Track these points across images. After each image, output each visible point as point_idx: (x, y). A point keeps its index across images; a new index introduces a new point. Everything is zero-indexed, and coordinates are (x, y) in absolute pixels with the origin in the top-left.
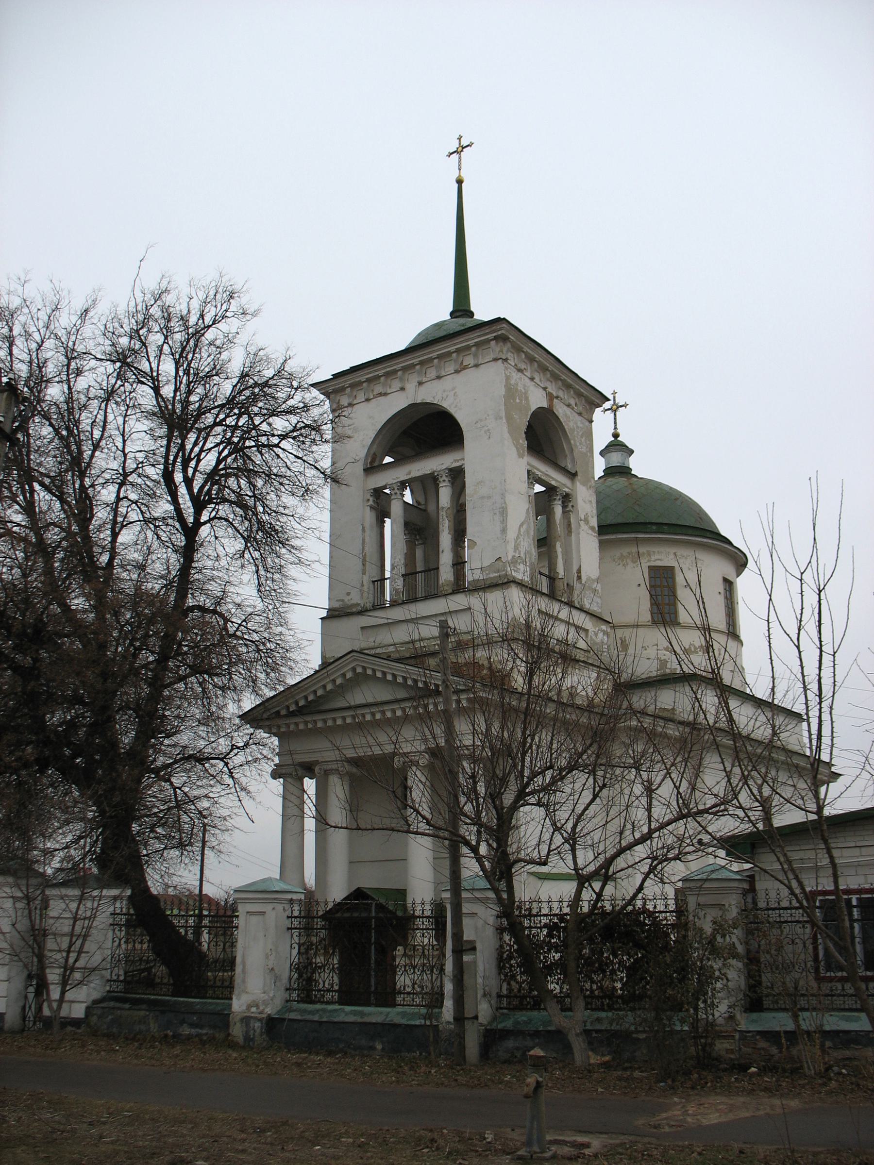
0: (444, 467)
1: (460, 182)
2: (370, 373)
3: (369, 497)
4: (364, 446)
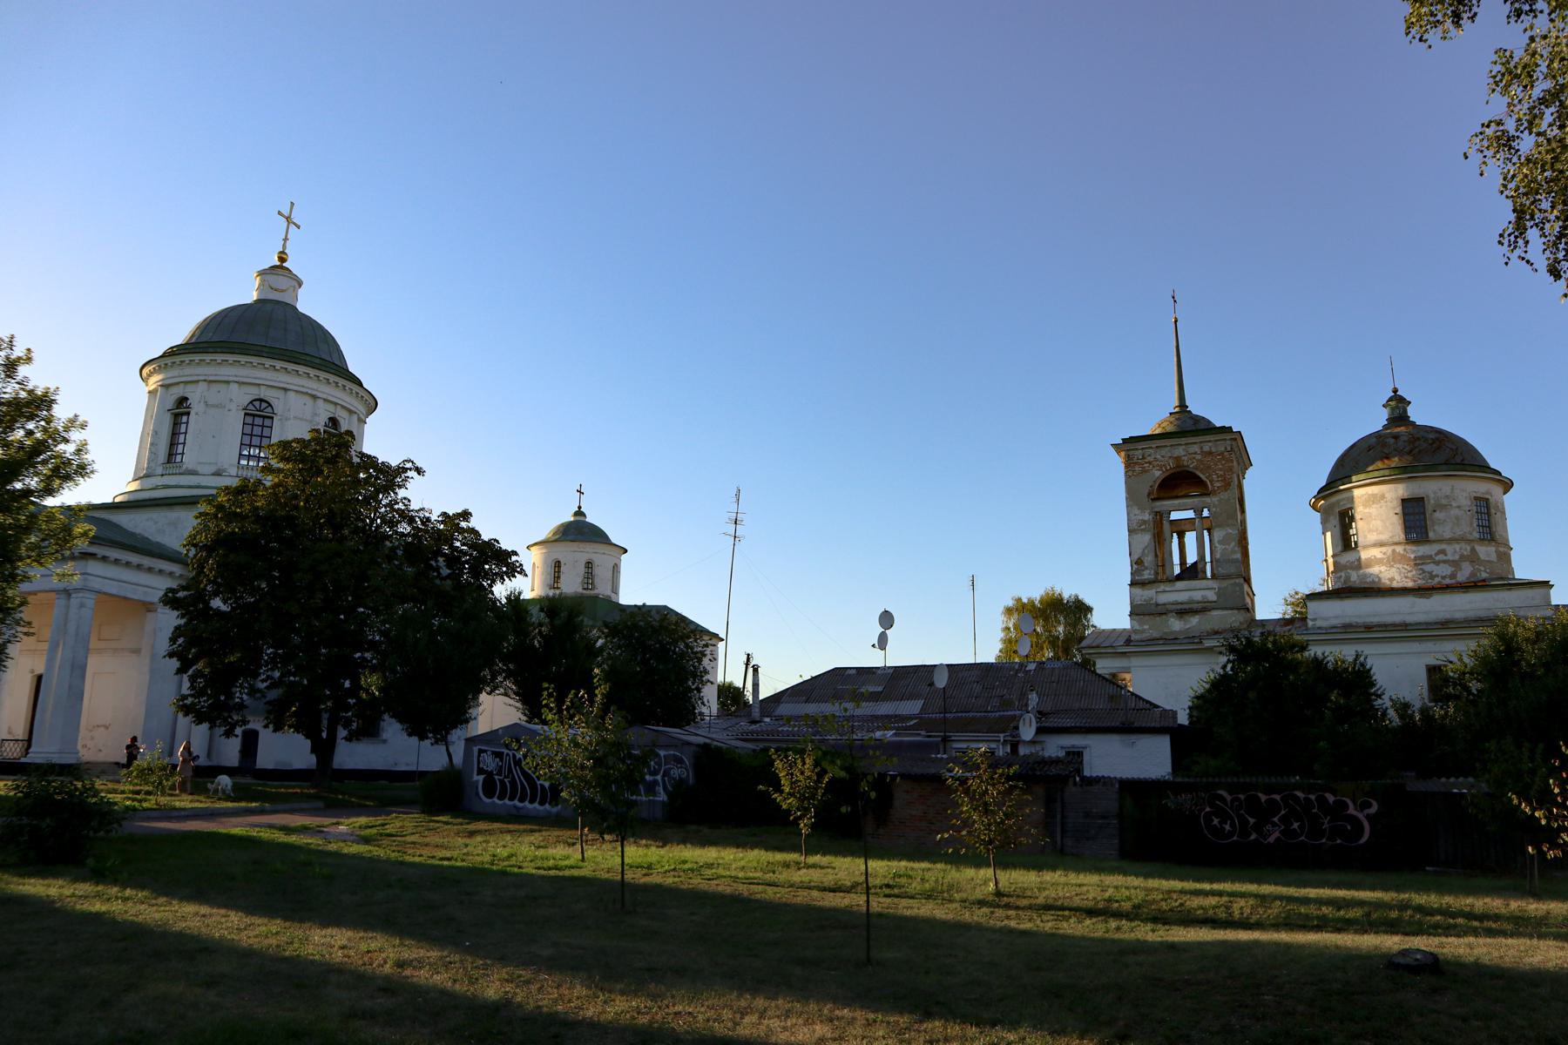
1: (1176, 321)
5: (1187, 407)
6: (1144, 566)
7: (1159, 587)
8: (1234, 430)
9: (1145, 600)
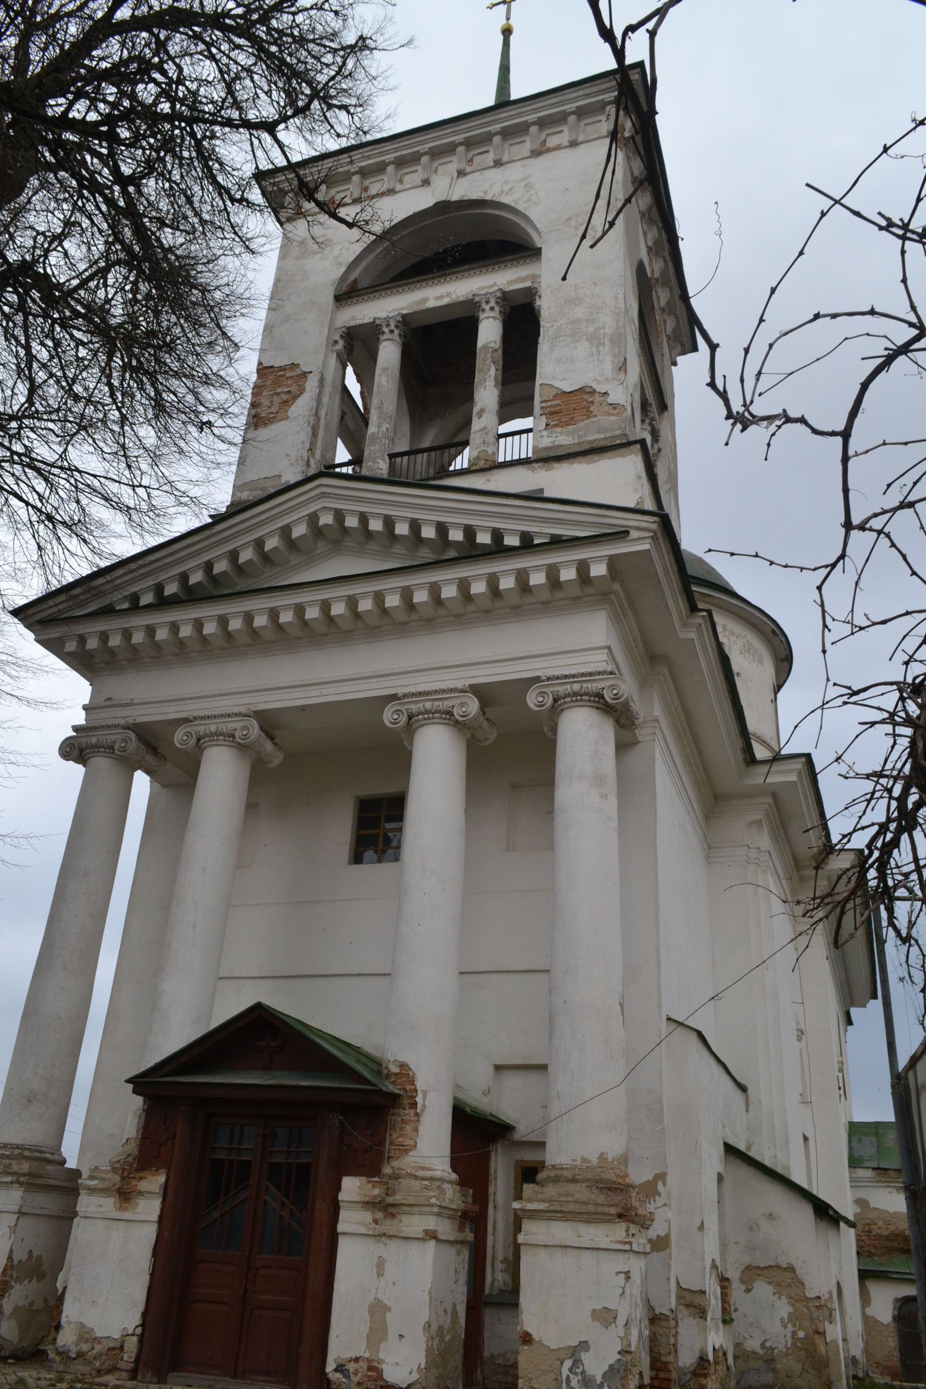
0: (496, 288)
2: (368, 157)
4: (340, 264)
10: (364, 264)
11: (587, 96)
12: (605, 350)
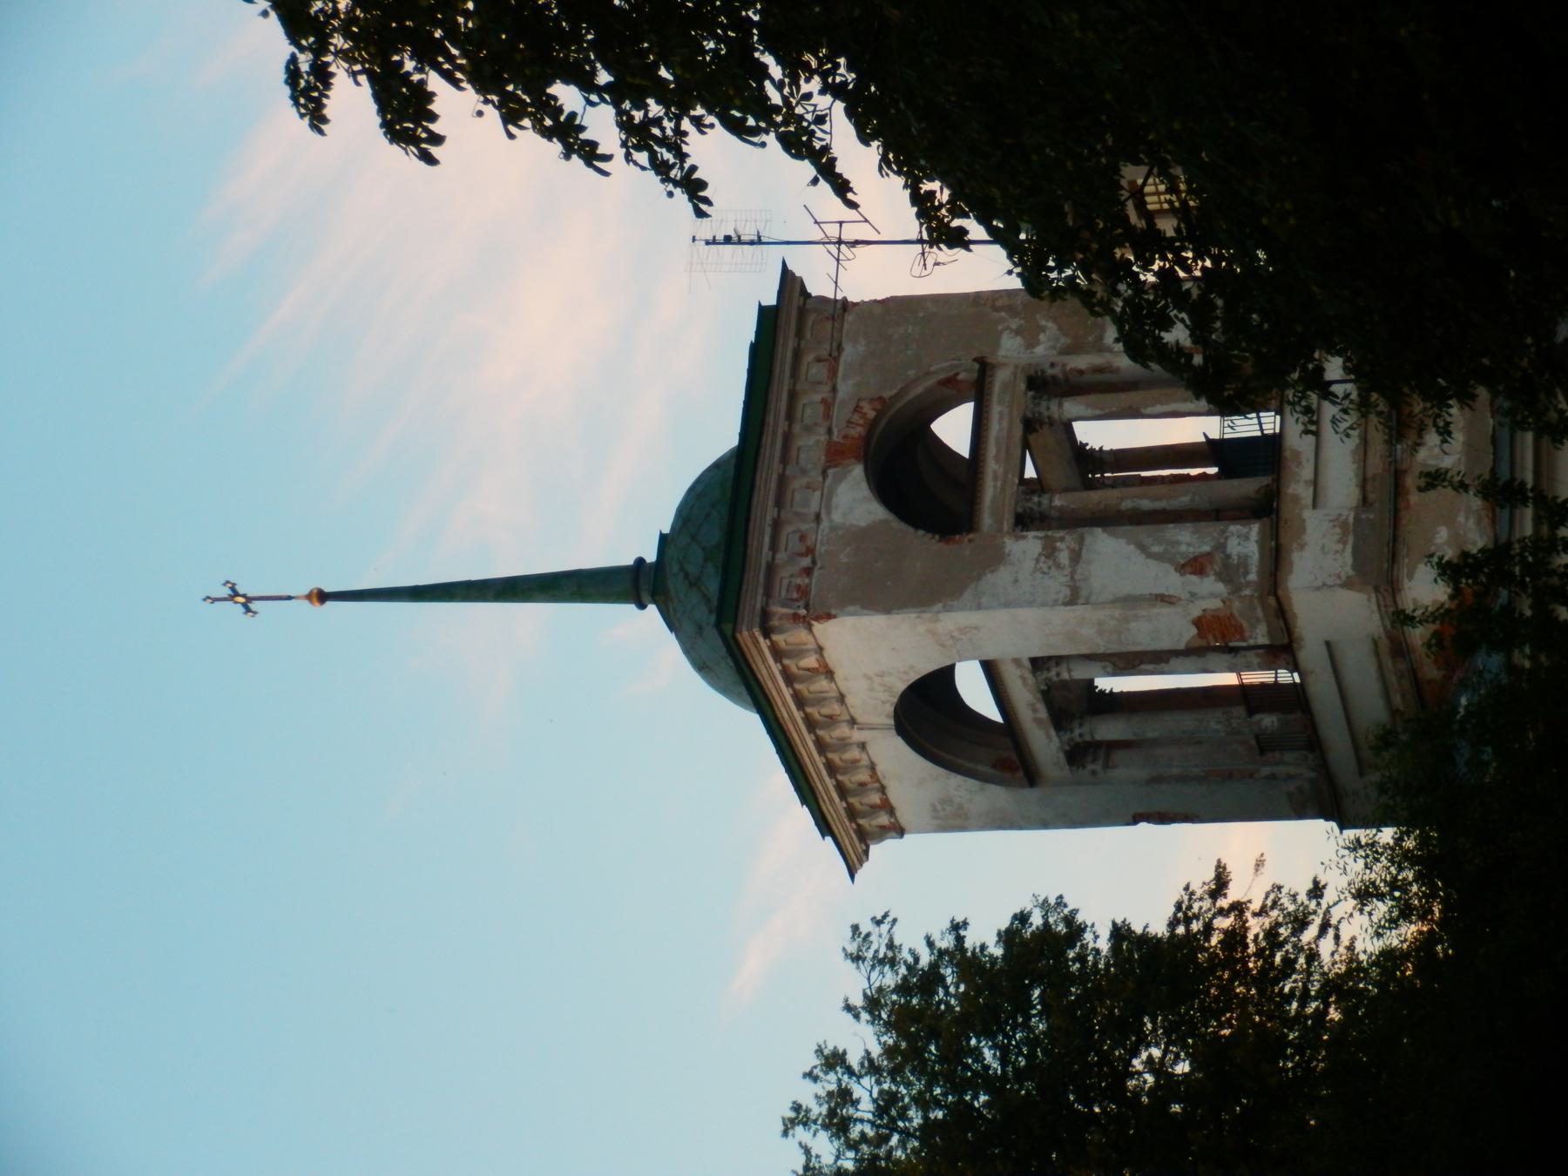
0: (1029, 676)
1: (322, 597)
2: (831, 800)
3: (1084, 773)
5: (640, 561)
6: (1209, 554)
7: (1296, 499)
8: (771, 300)
9: (1343, 541)
10: (971, 765)
11: (764, 660)
12: (1142, 612)
